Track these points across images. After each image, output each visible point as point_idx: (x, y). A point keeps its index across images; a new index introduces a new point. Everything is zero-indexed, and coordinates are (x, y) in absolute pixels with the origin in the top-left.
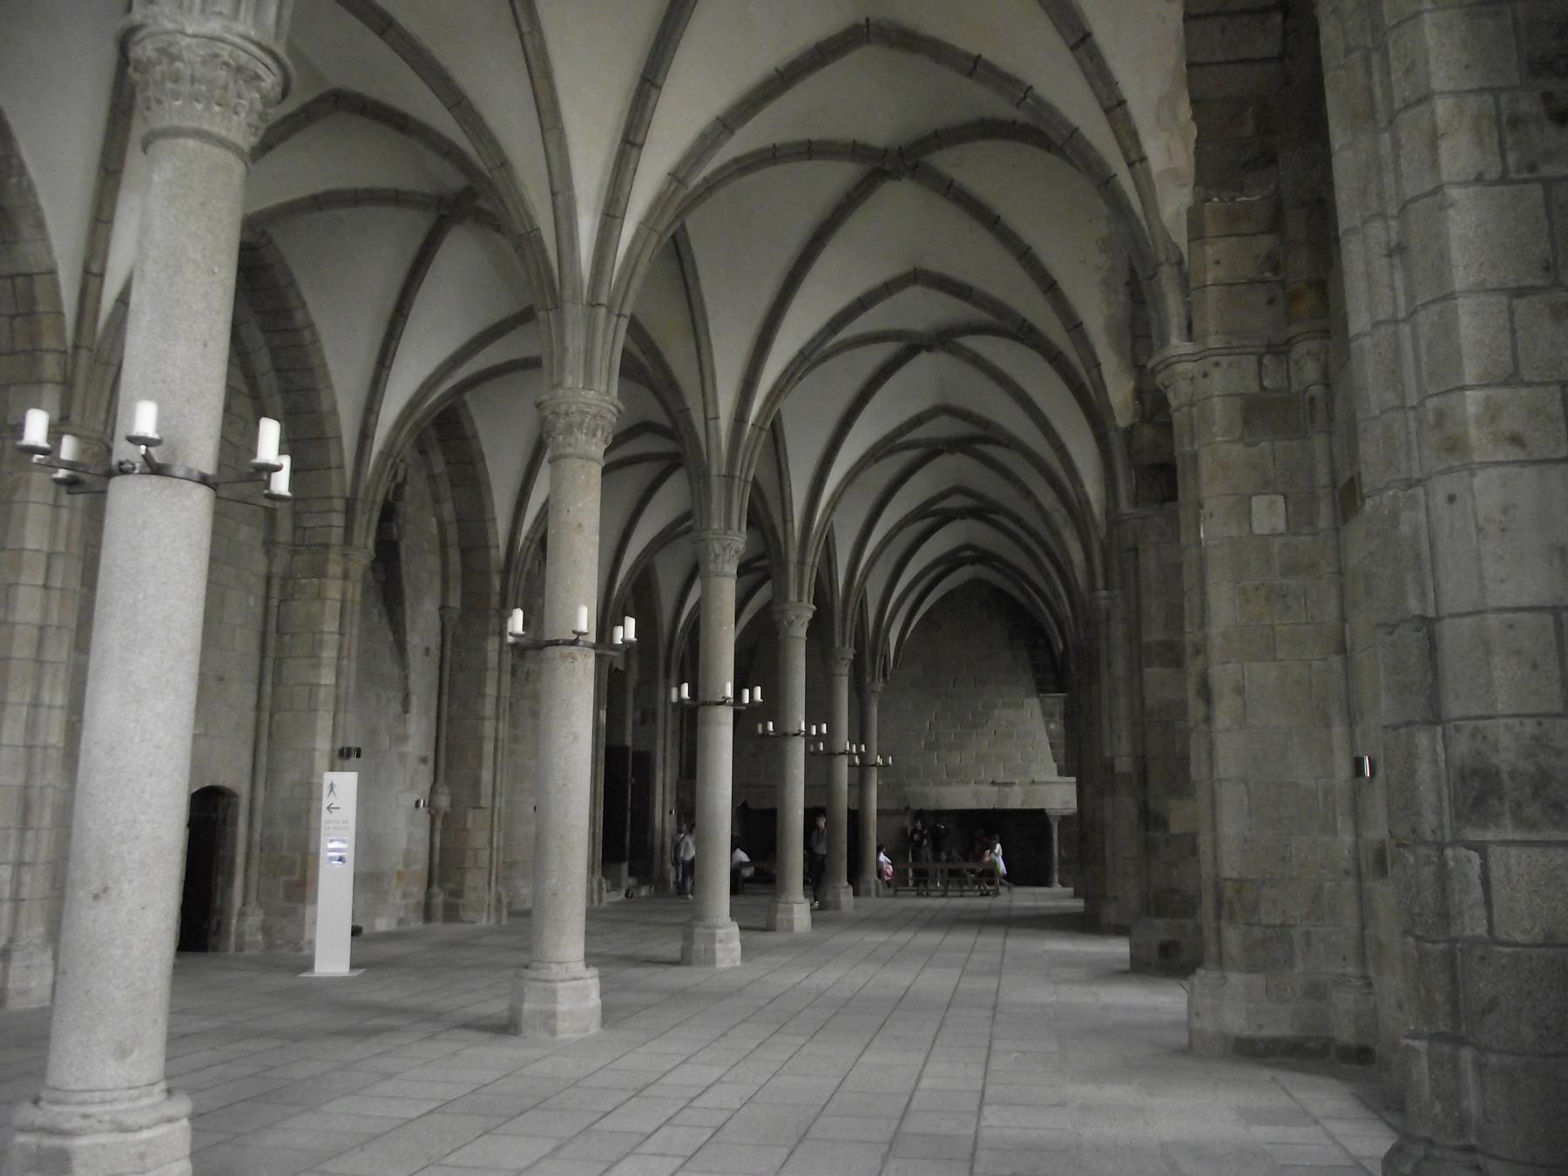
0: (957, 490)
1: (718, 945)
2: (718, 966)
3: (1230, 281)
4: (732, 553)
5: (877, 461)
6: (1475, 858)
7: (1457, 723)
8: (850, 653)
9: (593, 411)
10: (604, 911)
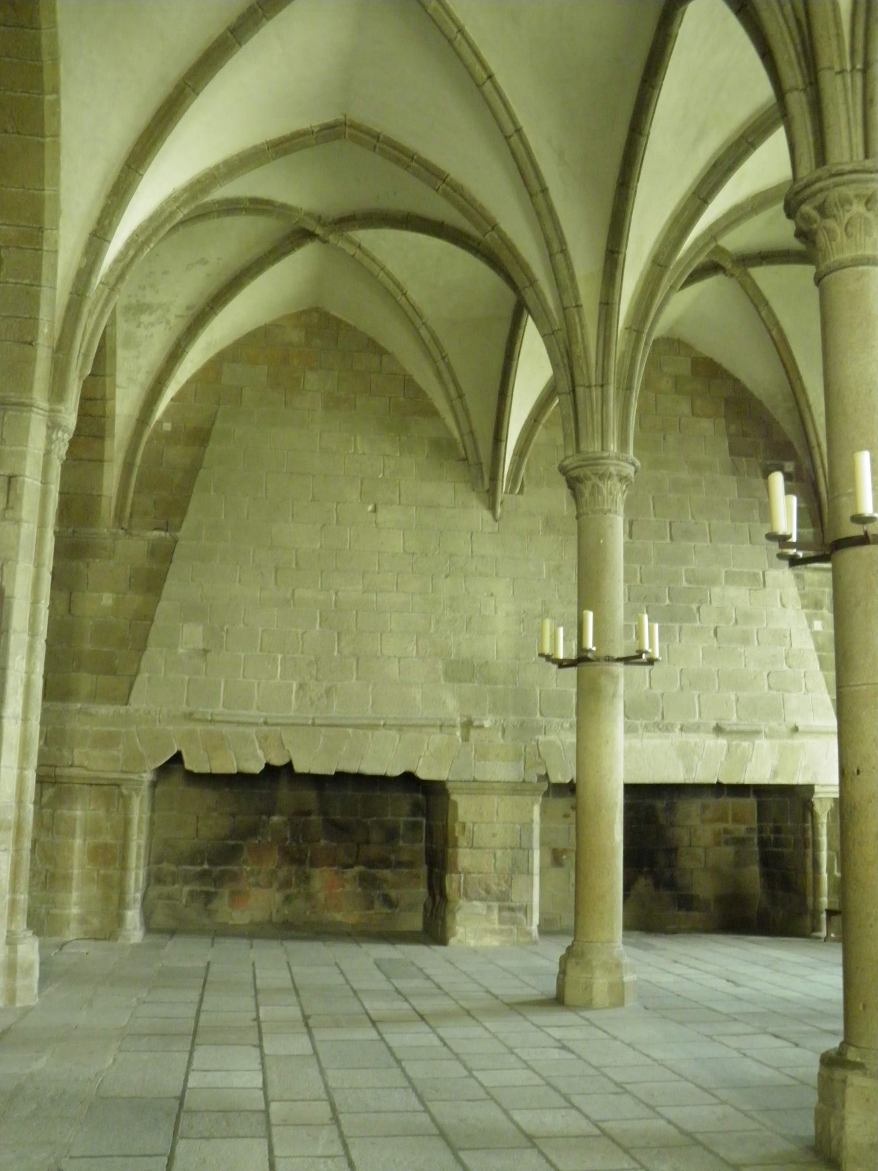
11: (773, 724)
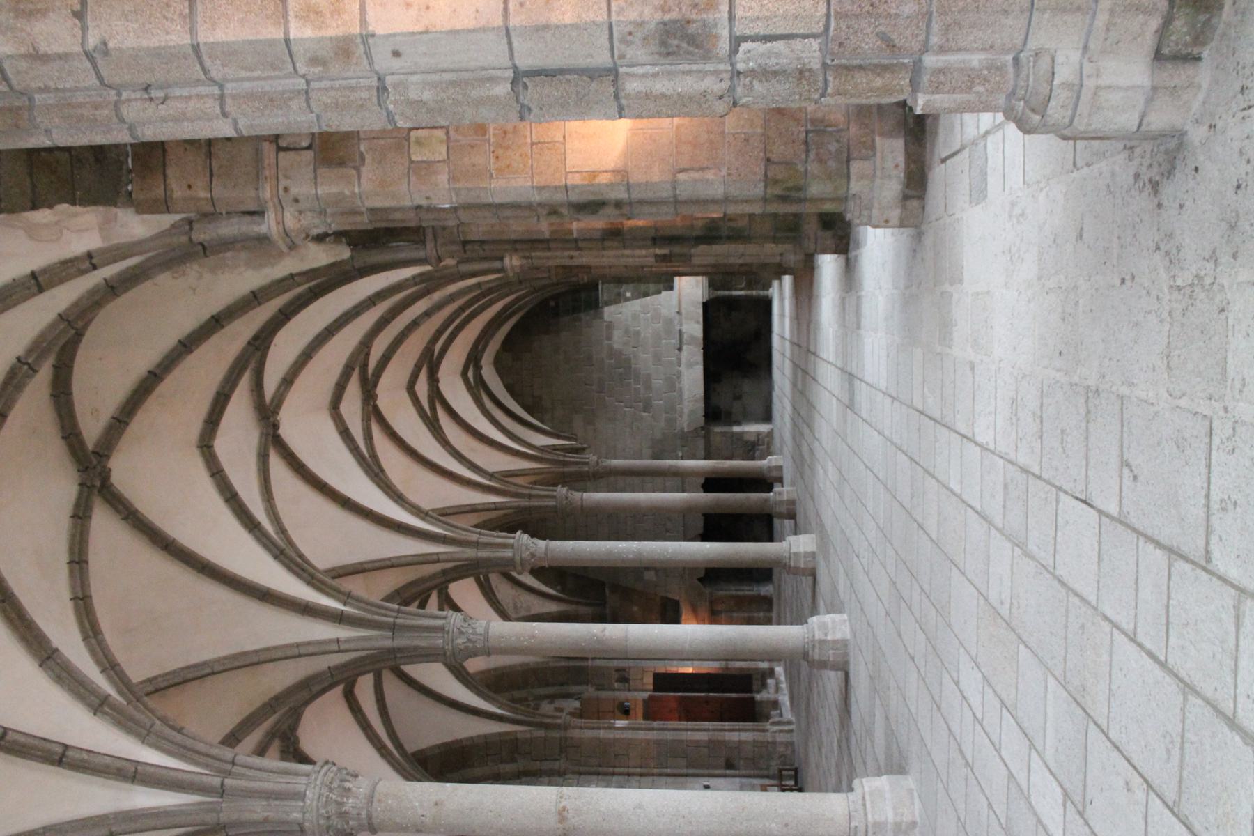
0: (411, 389)
1: (829, 638)
2: (849, 636)
3: (208, 174)
4: (466, 625)
5: (382, 471)
6: (744, 46)
7: (616, 57)
8: (562, 491)
9: (325, 791)
10: (798, 720)
11: (676, 322)
